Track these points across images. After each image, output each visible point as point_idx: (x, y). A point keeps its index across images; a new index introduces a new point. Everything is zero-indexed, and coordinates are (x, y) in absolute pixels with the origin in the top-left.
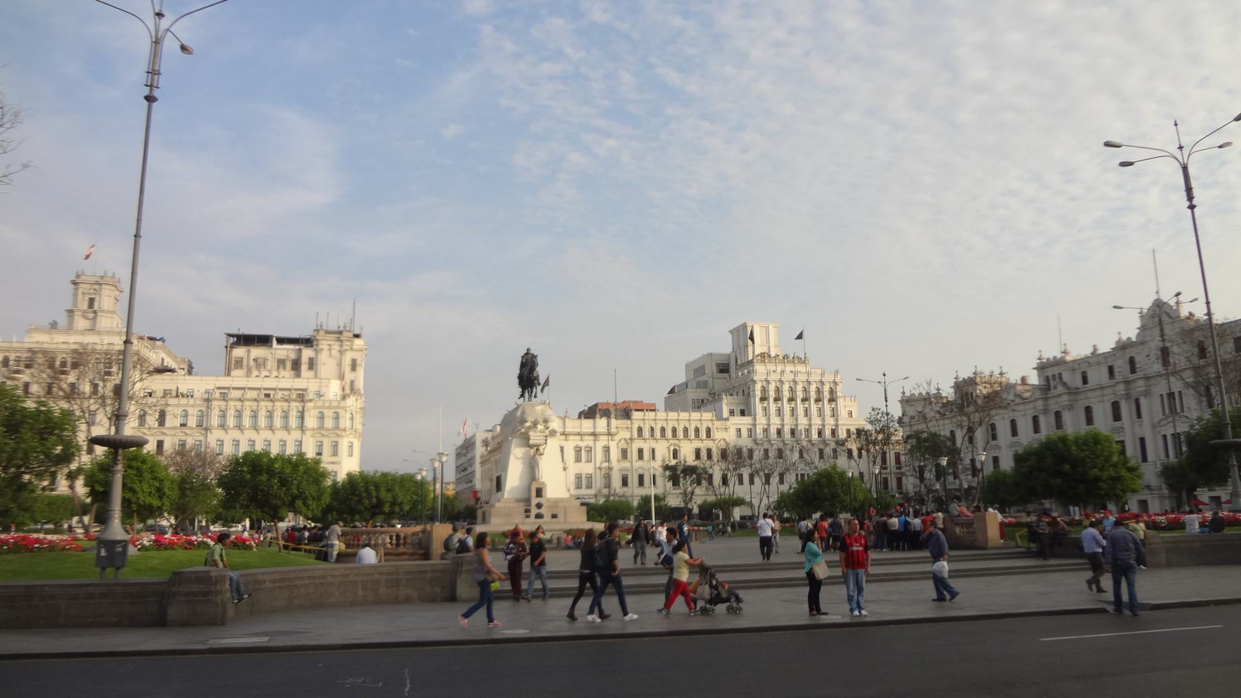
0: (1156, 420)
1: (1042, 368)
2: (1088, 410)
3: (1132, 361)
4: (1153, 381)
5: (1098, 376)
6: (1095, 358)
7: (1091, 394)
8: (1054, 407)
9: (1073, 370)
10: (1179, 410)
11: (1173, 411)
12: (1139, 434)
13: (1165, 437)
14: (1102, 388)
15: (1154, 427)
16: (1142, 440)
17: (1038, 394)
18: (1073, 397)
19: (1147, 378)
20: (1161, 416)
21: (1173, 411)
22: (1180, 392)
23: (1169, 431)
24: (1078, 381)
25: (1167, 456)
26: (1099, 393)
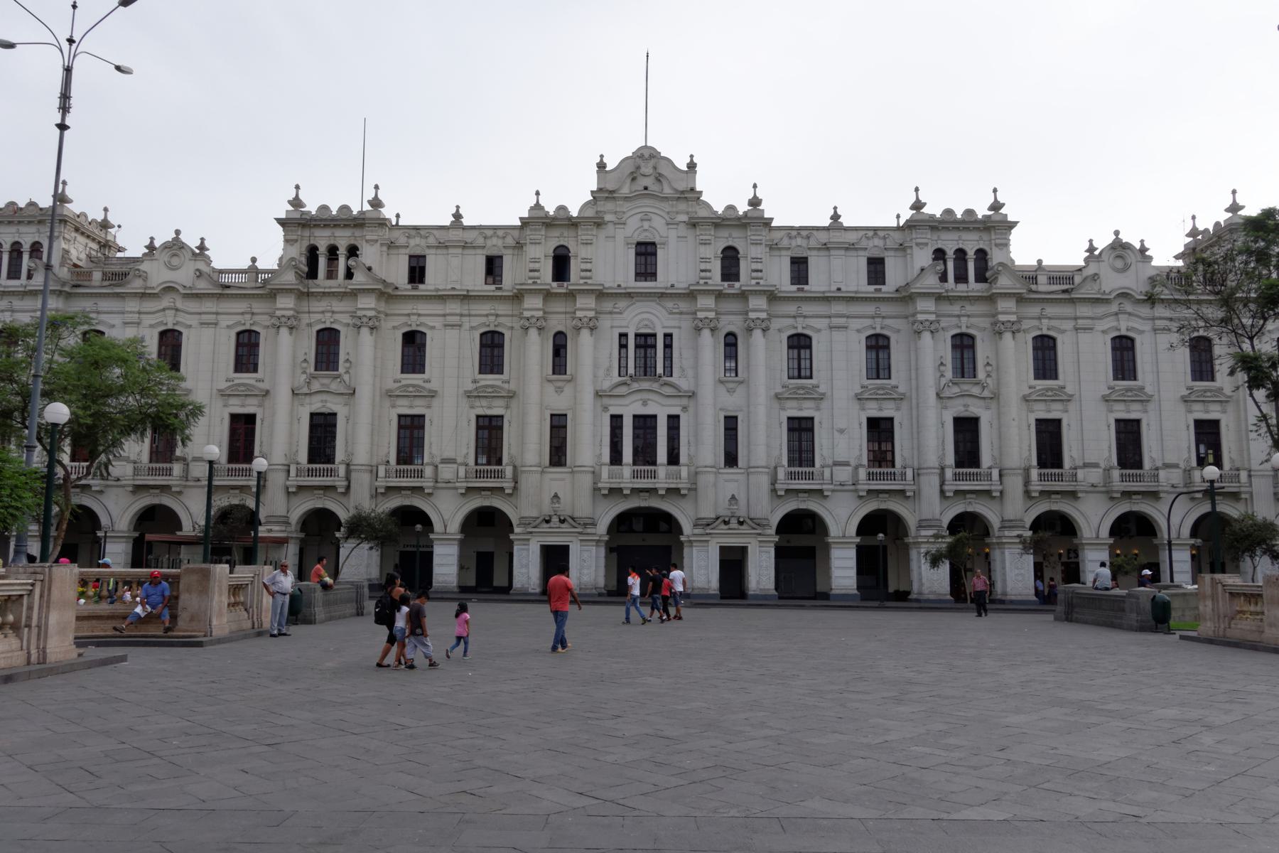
0: (606, 385)
1: (297, 223)
2: (413, 342)
4: (608, 305)
5: (454, 272)
6: (456, 235)
7: (423, 308)
9: (391, 246)
10: (660, 370)
11: (646, 369)
12: (559, 404)
13: (616, 420)
14: (466, 298)
15: (598, 395)
16: (558, 425)
17: (290, 278)
18: (382, 306)
19: (601, 295)
20: (616, 379)
21: (646, 369)
22: (668, 336)
23: (629, 409)
24: (398, 272)
25: (616, 458)
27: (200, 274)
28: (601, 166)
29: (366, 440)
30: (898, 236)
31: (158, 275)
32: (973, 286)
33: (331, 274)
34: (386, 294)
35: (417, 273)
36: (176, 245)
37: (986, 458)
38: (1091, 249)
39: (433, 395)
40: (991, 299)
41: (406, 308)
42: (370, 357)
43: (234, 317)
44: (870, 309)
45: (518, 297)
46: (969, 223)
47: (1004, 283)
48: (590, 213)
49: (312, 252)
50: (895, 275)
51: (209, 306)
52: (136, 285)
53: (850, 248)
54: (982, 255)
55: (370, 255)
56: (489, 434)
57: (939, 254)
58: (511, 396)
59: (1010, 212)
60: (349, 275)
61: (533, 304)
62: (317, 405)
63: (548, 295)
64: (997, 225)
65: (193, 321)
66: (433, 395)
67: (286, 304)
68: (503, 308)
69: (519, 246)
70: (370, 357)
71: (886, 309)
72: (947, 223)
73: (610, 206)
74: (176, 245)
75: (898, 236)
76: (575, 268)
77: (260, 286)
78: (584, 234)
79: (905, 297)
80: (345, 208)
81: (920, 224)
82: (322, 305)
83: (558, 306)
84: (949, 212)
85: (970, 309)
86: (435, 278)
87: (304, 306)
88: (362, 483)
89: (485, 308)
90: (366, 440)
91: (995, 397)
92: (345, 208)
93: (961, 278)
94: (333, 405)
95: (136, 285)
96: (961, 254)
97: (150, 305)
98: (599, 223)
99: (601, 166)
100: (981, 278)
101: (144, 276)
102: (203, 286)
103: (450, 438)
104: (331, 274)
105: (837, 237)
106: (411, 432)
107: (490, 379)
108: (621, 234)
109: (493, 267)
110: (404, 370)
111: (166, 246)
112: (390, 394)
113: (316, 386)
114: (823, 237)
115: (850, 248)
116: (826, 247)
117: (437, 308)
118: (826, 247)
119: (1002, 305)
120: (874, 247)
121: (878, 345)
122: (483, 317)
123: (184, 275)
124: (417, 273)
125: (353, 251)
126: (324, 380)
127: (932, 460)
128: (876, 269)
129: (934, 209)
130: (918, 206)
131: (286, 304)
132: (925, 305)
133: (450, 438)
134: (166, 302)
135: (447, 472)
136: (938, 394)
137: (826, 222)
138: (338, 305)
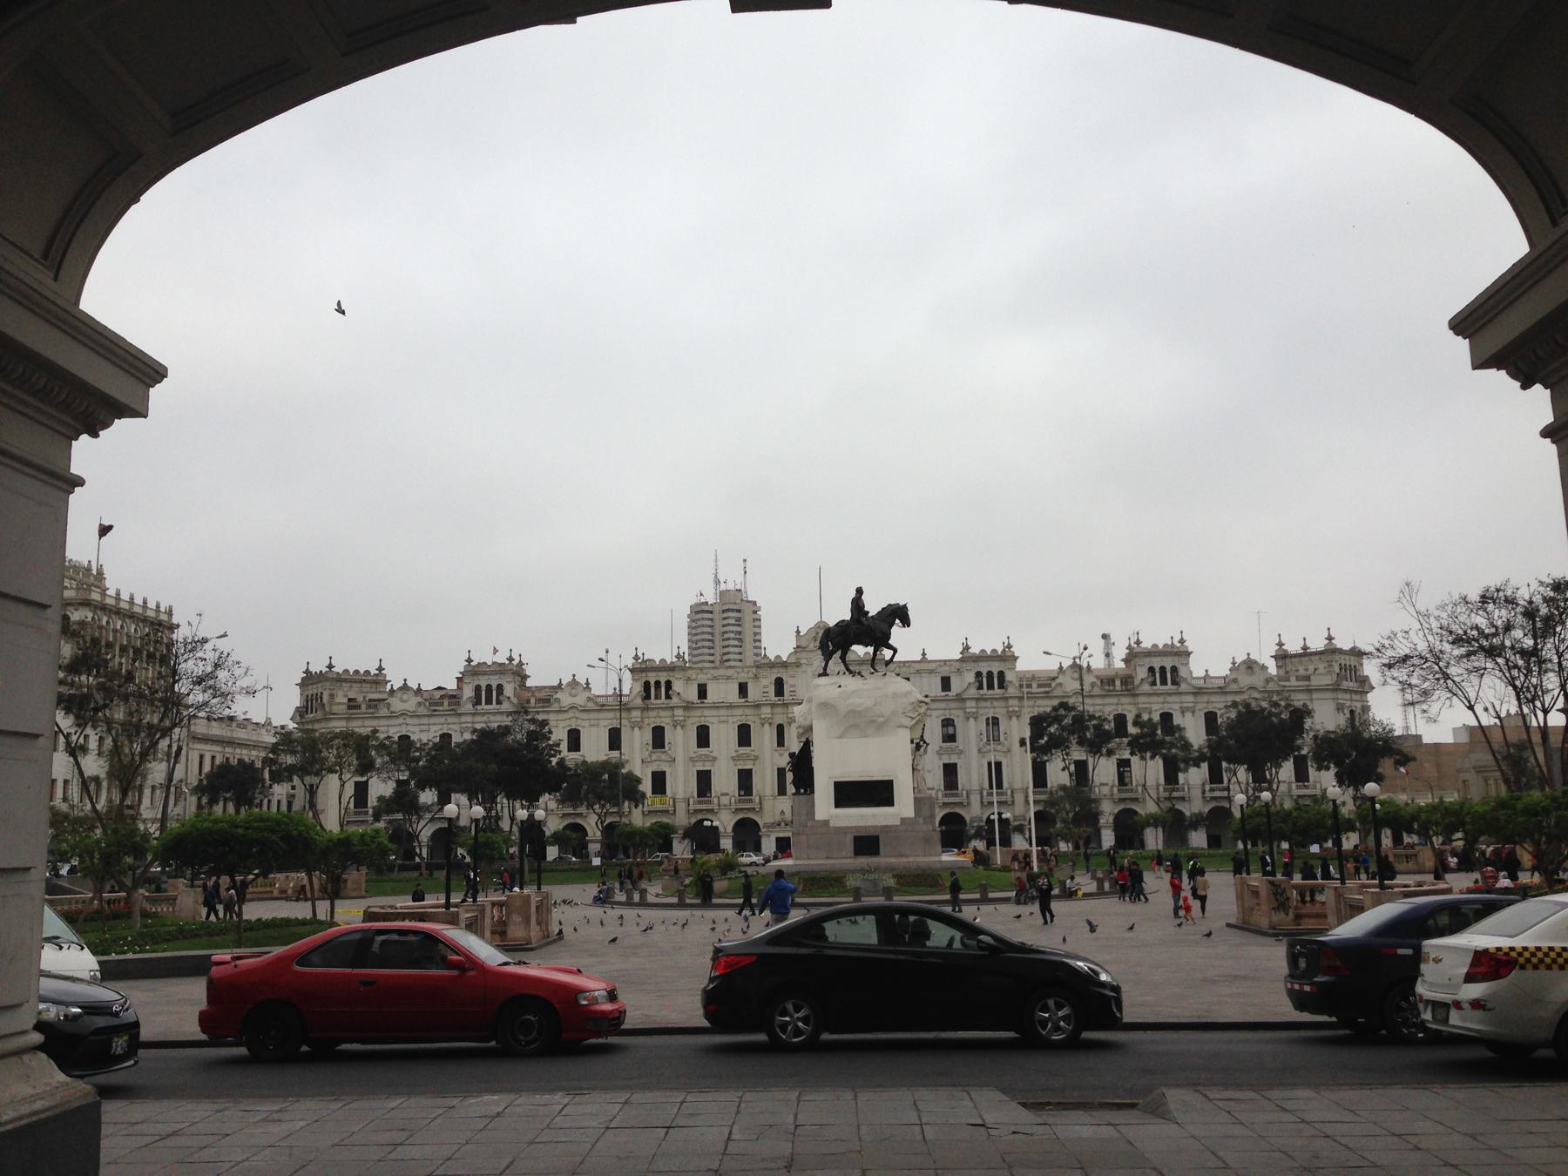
3: (779, 684)
7: (707, 712)
8: (653, 720)
14: (731, 706)
17: (639, 701)
24: (692, 694)
26: (723, 712)
27: (589, 699)
28: (798, 632)
29: (681, 785)
30: (957, 665)
31: (565, 699)
32: (997, 691)
33: (657, 697)
34: (688, 707)
35: (702, 692)
36: (574, 683)
37: (1005, 785)
38: (1061, 668)
39: (715, 759)
40: (1006, 699)
41: (698, 713)
42: (681, 741)
43: (608, 720)
44: (943, 705)
45: (757, 706)
46: (994, 657)
47: (1012, 691)
48: (793, 660)
49: (647, 684)
50: (957, 686)
51: (593, 715)
52: (555, 707)
53: (931, 672)
54: (1001, 674)
55: (677, 686)
56: (745, 778)
57: (979, 674)
58: (756, 758)
59: (1016, 650)
60: (668, 697)
61: (766, 711)
62: (655, 767)
63: (773, 706)
64: (1007, 656)
65: (586, 724)
66: (715, 759)
67: (636, 714)
68: (749, 711)
69: (756, 677)
70: (681, 741)
71: (952, 705)
72: (982, 657)
73: (804, 655)
74: (574, 683)
75: (957, 665)
76: (786, 689)
77: (620, 704)
78: (791, 671)
79: (960, 699)
80: (663, 661)
81: (967, 657)
82: (654, 713)
83: (779, 710)
84: (983, 651)
85: (996, 703)
86: (713, 694)
87: (646, 714)
88: (681, 807)
89: (739, 712)
90: (681, 785)
91: (1009, 750)
92: (663, 661)
93: (990, 687)
94: (664, 767)
95: (555, 707)
96: (990, 674)
97: (561, 716)
98: (798, 665)
99: (798, 632)
100: (1001, 686)
101: (558, 700)
102: (591, 705)
103: (725, 783)
104: (657, 697)
105: (925, 666)
106: (704, 780)
107: (745, 750)
108: (810, 670)
109: (743, 689)
110: (699, 746)
111: (569, 684)
112: (692, 759)
113: (654, 757)
114: (918, 666)
115: (931, 672)
116: (918, 672)
117: (714, 712)
118: (918, 672)
119: (1011, 702)
120: (945, 671)
121: (947, 722)
122: (739, 717)
123: (580, 700)
124: (702, 692)
125: (669, 684)
126: (658, 754)
127: (975, 786)
128: (946, 684)
129: (975, 650)
130: (967, 648)
131: (636, 714)
132: (970, 704)
133: (725, 783)
134: (570, 714)
135: (725, 800)
136: (979, 751)
137: (919, 658)
138: (662, 713)
